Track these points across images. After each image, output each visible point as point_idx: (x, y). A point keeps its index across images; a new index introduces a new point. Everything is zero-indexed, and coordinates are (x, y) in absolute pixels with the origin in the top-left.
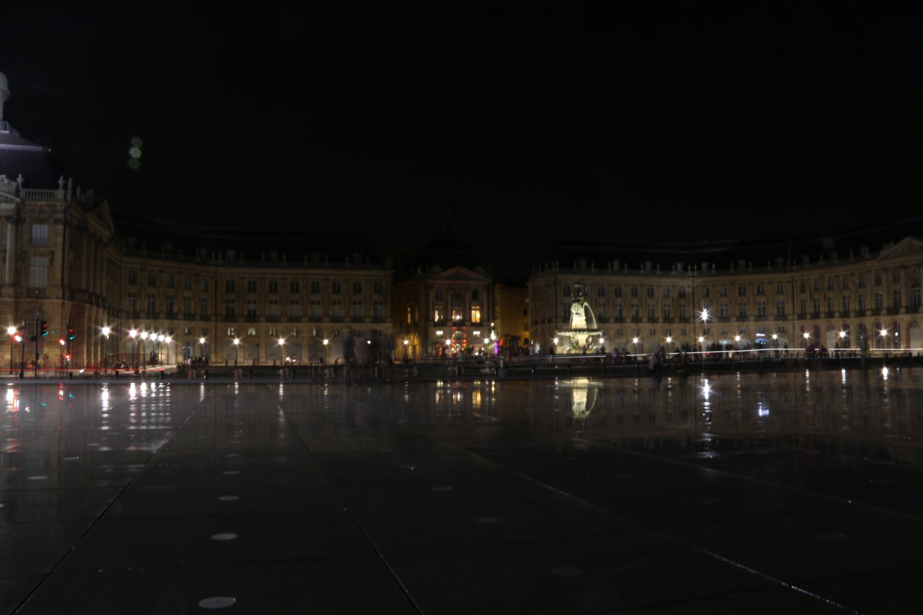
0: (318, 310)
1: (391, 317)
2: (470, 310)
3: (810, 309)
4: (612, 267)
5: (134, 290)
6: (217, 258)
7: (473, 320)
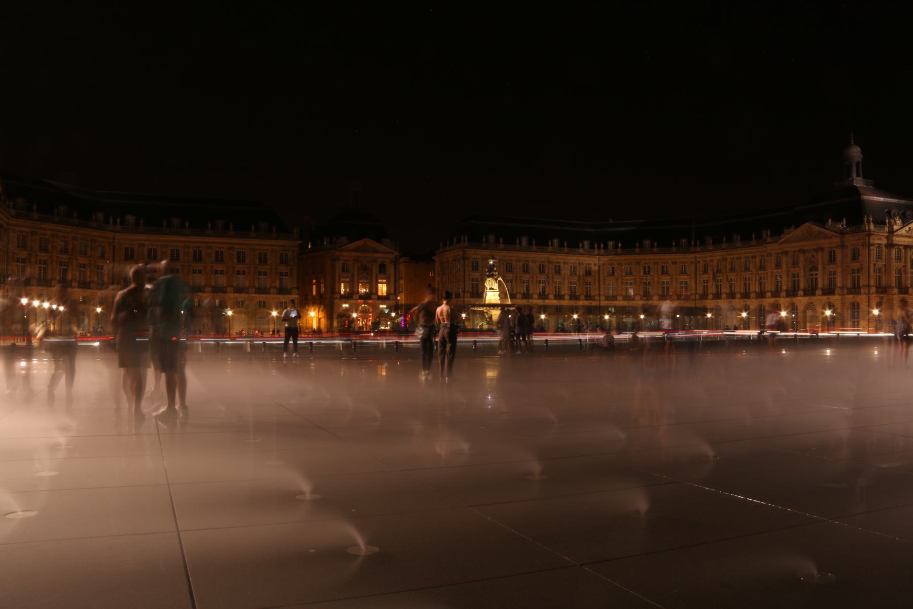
0: (222, 280)
1: (297, 288)
2: (377, 283)
3: (712, 290)
4: (520, 244)
5: (23, 254)
6: (115, 223)
7: (380, 294)
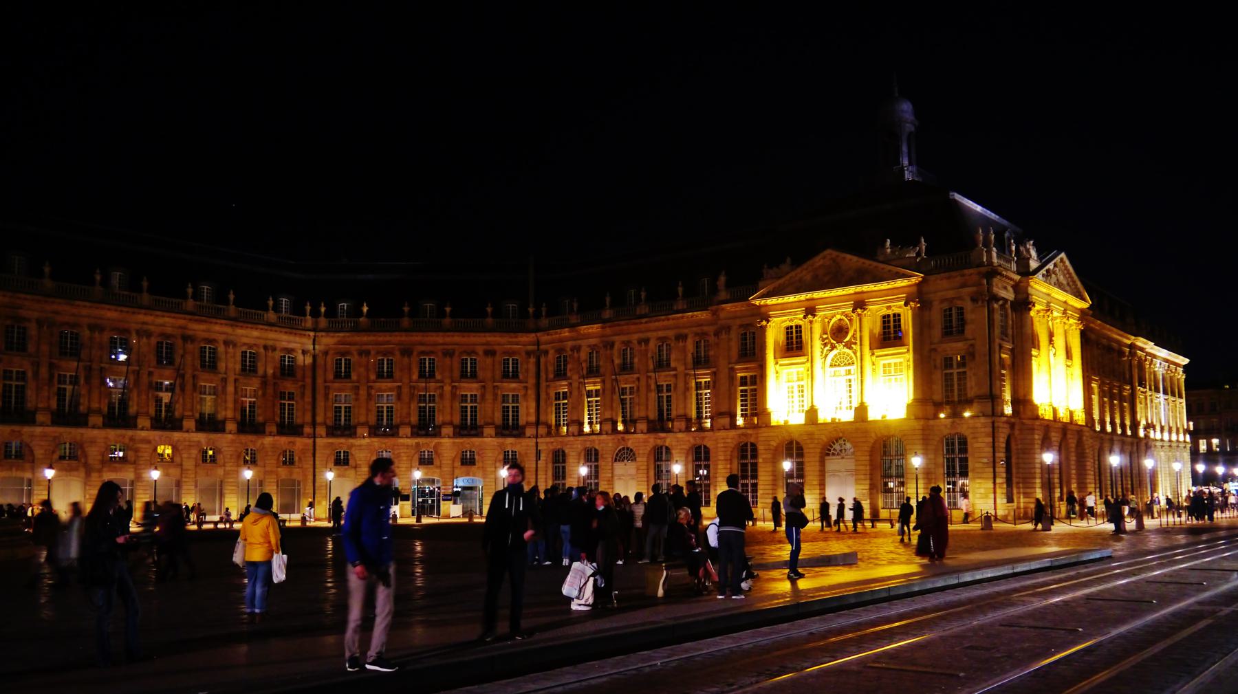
4: (106, 282)
